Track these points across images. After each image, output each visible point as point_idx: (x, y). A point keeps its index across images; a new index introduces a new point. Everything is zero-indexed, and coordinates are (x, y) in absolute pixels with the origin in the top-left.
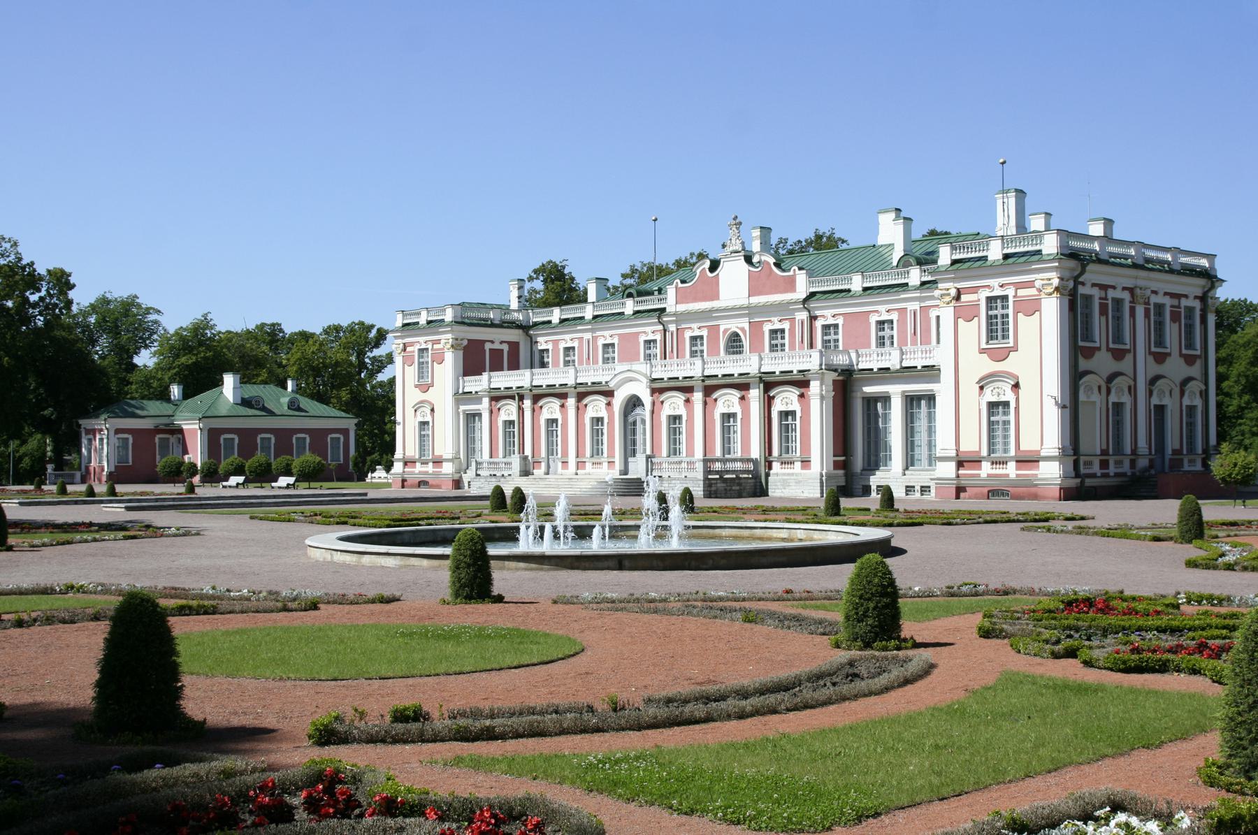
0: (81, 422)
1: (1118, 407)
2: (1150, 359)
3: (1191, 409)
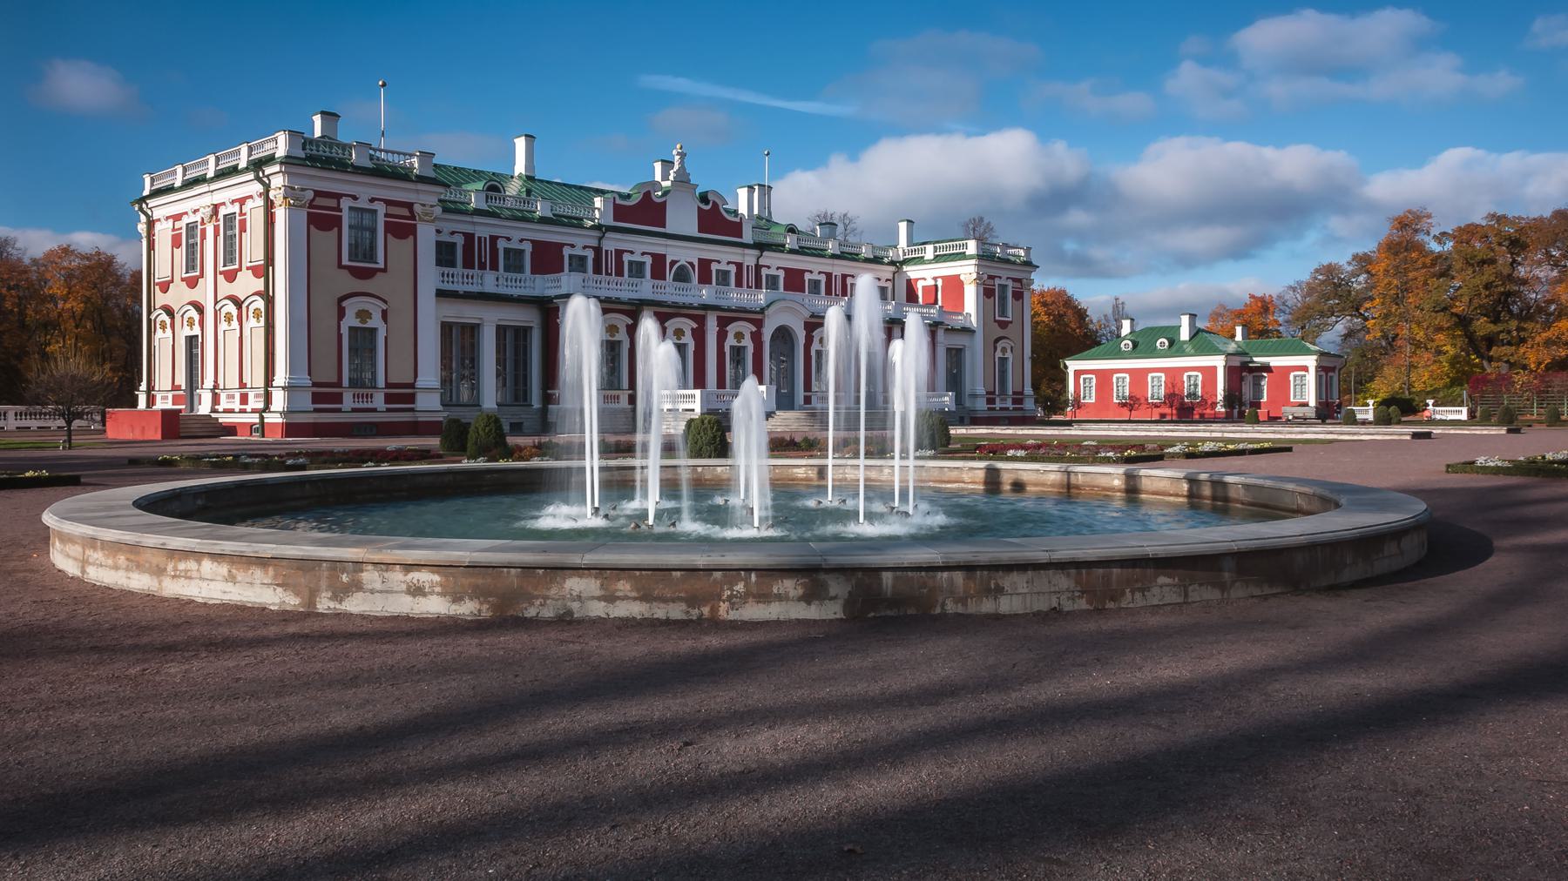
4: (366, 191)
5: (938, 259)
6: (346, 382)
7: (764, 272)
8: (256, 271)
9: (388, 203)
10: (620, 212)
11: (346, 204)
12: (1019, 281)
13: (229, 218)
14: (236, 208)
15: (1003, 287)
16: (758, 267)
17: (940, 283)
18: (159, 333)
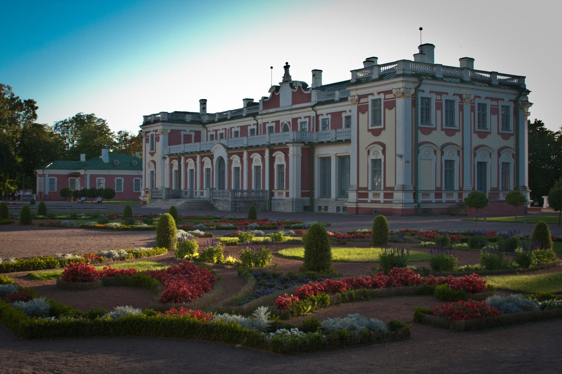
0: (37, 171)
1: (450, 163)
2: (475, 136)
3: (506, 165)
7: (321, 118)
16: (317, 116)
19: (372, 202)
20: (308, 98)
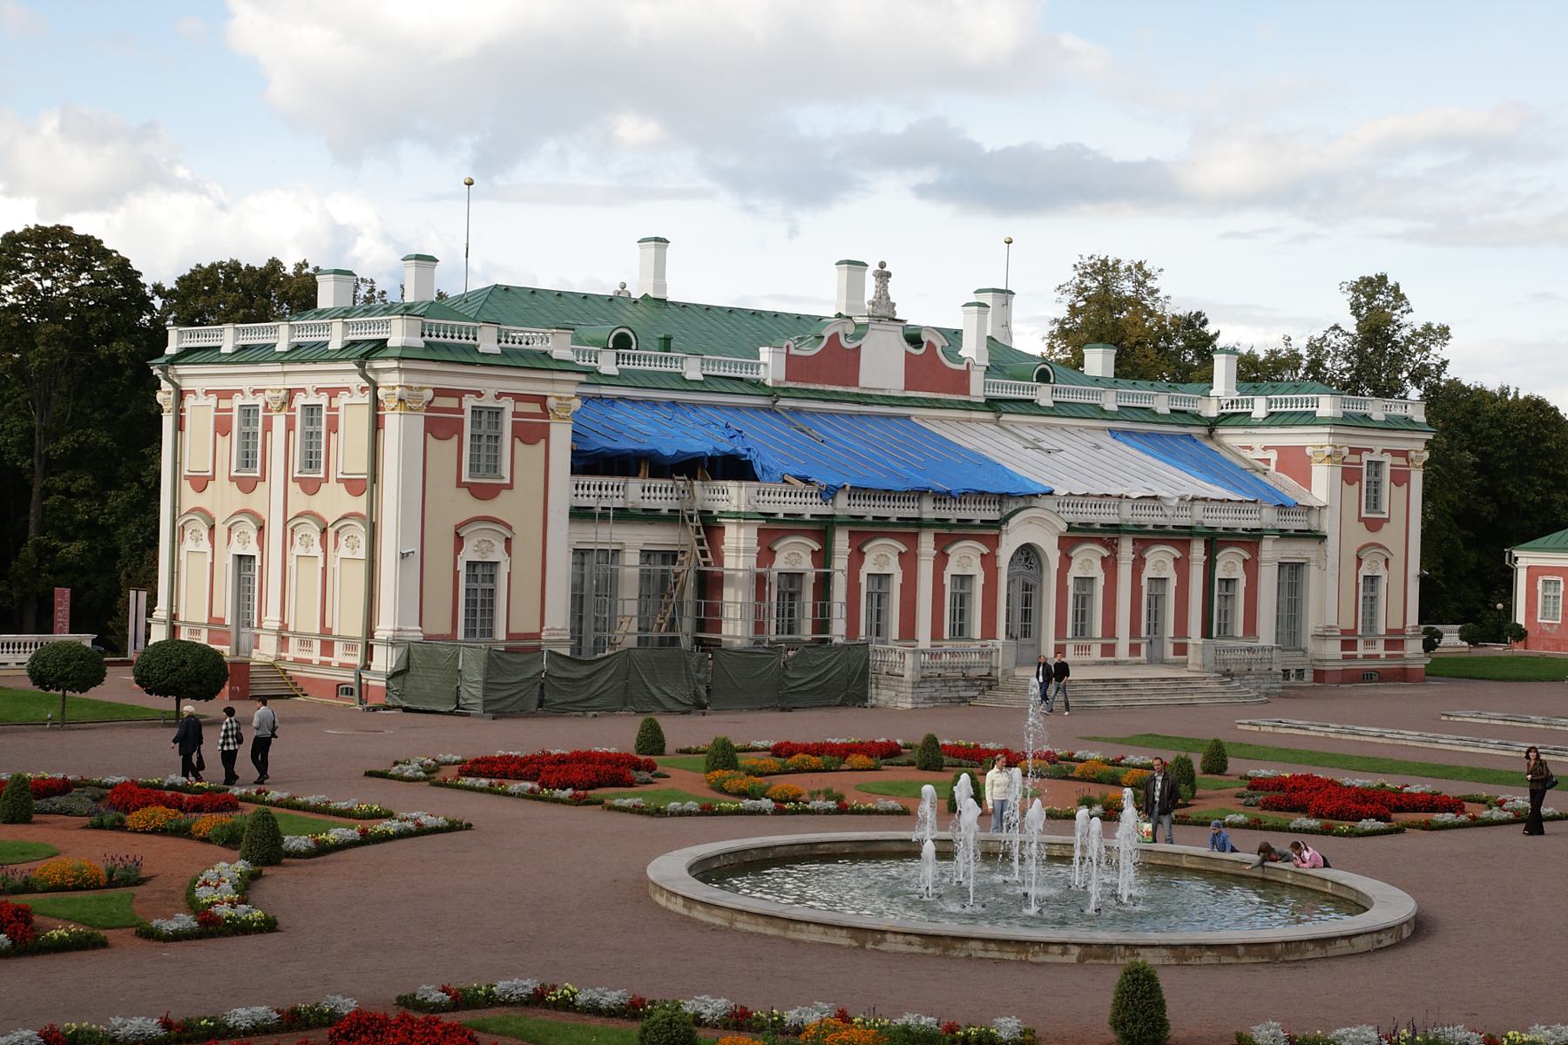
4: (490, 387)
5: (1273, 419)
6: (461, 635)
8: (354, 487)
9: (519, 398)
10: (795, 366)
11: (469, 402)
12: (1405, 454)
13: (311, 410)
14: (323, 400)
15: (1378, 464)
17: (1273, 456)
18: (188, 545)
19: (1366, 657)
20: (961, 380)
